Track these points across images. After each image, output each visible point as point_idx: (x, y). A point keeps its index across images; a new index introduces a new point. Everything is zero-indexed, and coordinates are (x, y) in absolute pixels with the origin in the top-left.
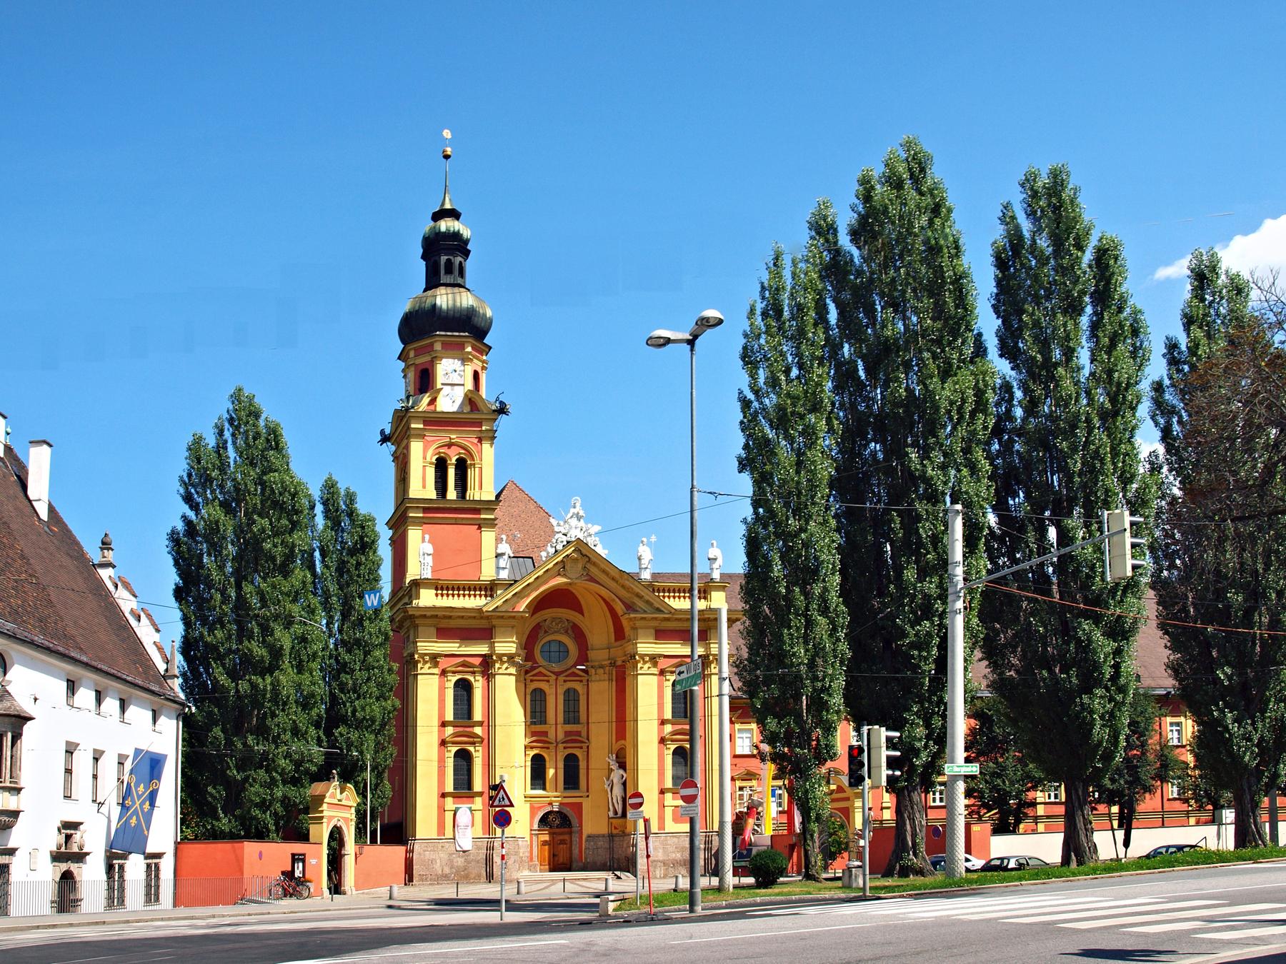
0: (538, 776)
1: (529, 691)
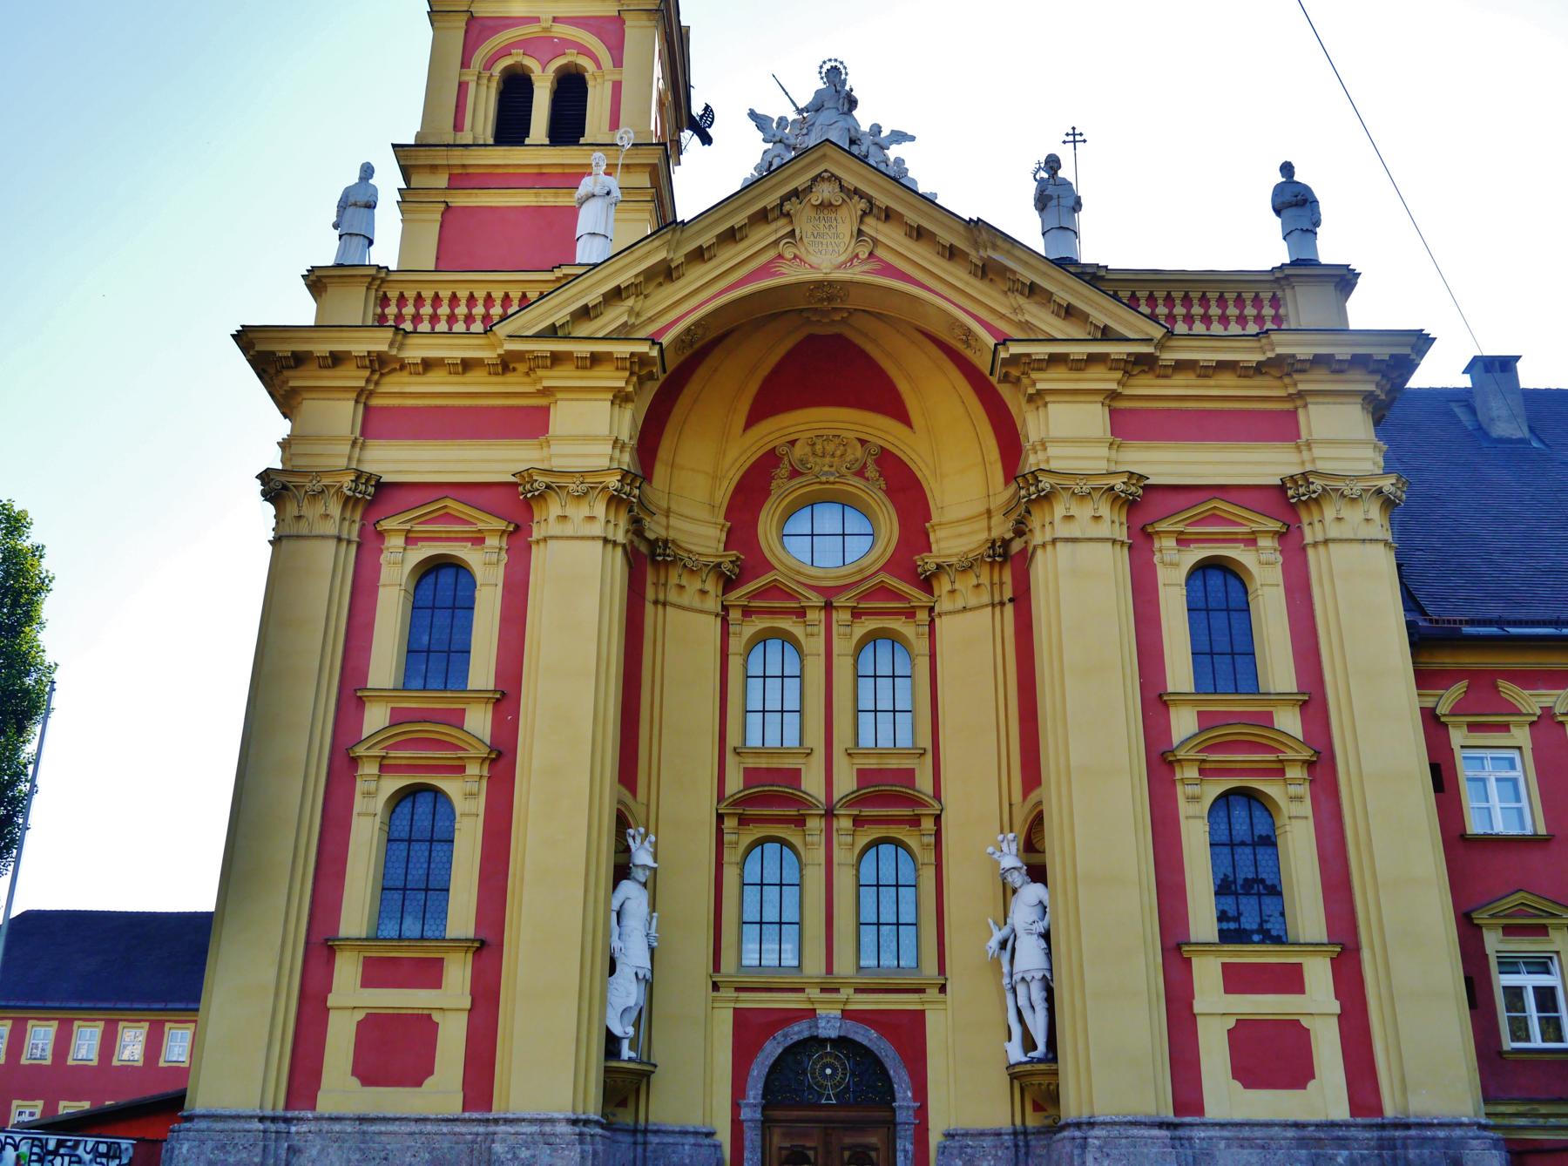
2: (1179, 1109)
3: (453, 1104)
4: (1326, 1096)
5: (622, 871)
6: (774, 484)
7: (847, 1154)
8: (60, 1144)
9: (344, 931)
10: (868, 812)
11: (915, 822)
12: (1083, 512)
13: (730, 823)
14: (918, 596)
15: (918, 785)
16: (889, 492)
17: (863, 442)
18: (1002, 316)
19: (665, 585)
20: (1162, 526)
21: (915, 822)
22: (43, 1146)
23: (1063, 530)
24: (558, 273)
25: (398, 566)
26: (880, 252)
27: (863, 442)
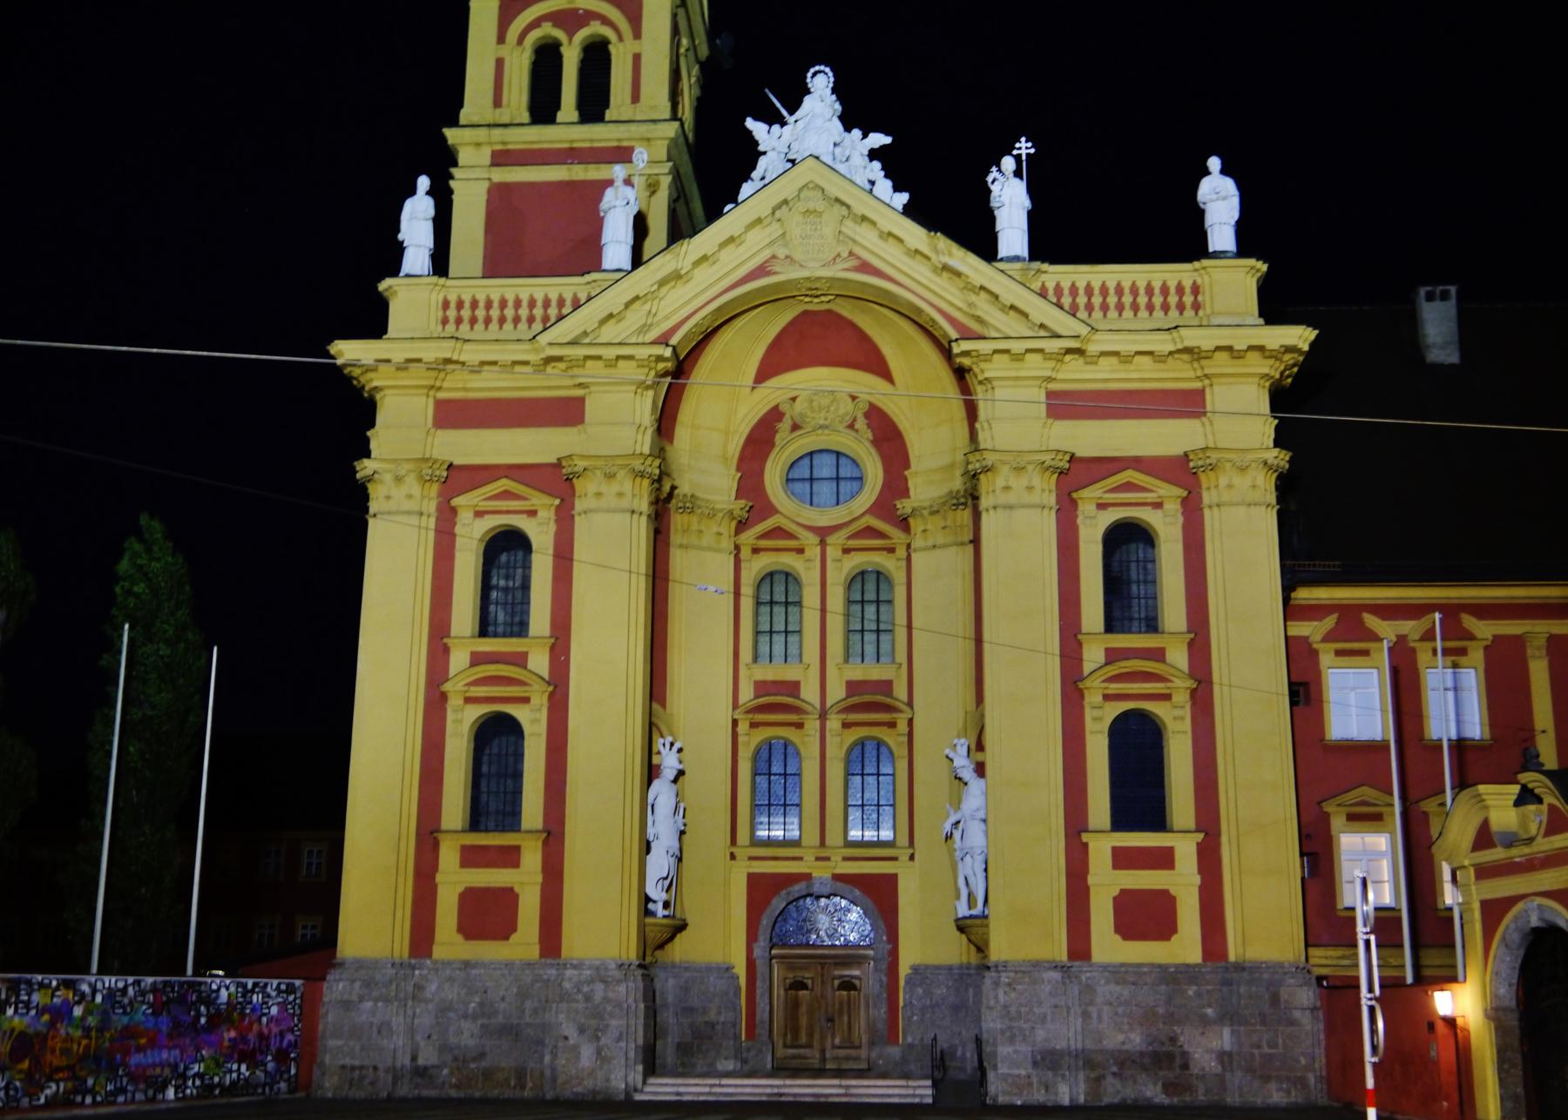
2: (1073, 955)
3: (534, 952)
4: (1186, 947)
5: (651, 772)
6: (778, 436)
7: (836, 982)
8: (255, 985)
9: (445, 825)
10: (853, 717)
11: (892, 725)
12: (1019, 483)
13: (743, 727)
14: (897, 535)
15: (895, 694)
17: (854, 398)
18: (960, 309)
20: (1085, 493)
21: (892, 725)
22: (244, 986)
23: (1002, 498)
24: (588, 278)
25: (471, 535)
26: (858, 251)
27: (854, 398)
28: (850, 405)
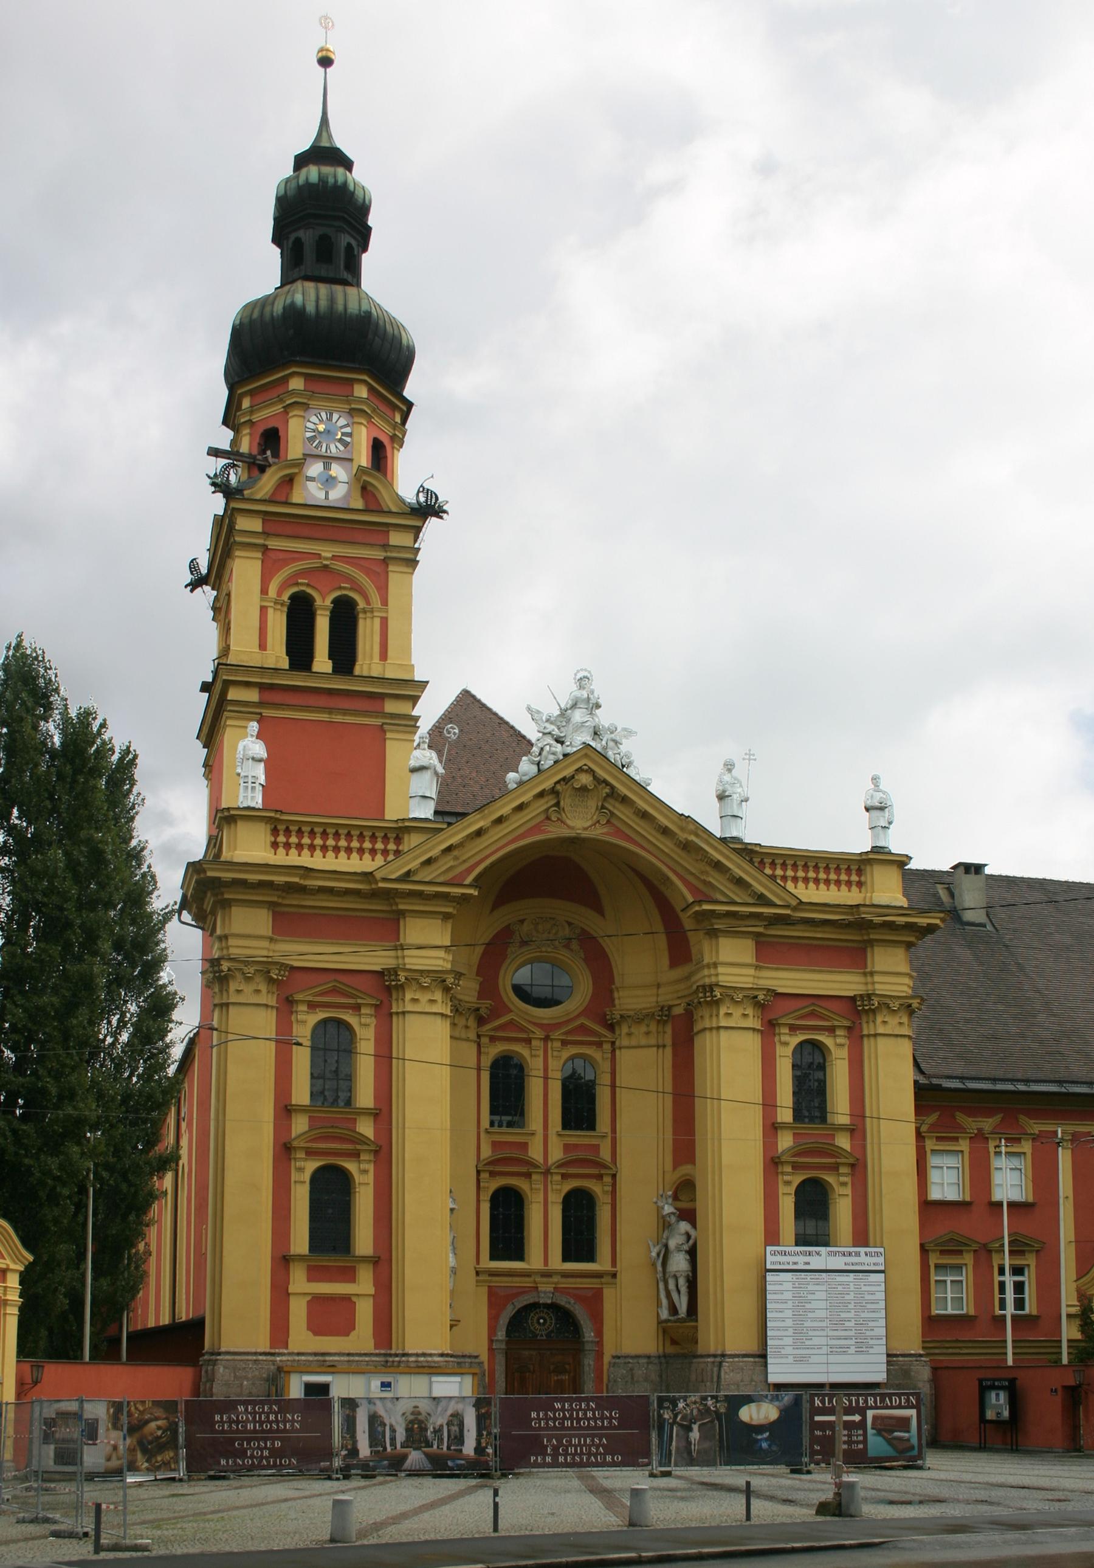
0: (506, 1229)
1: (487, 1062)
16: (586, 960)
17: (570, 924)
19: (403, 1000)
27: (570, 924)
28: (567, 932)
